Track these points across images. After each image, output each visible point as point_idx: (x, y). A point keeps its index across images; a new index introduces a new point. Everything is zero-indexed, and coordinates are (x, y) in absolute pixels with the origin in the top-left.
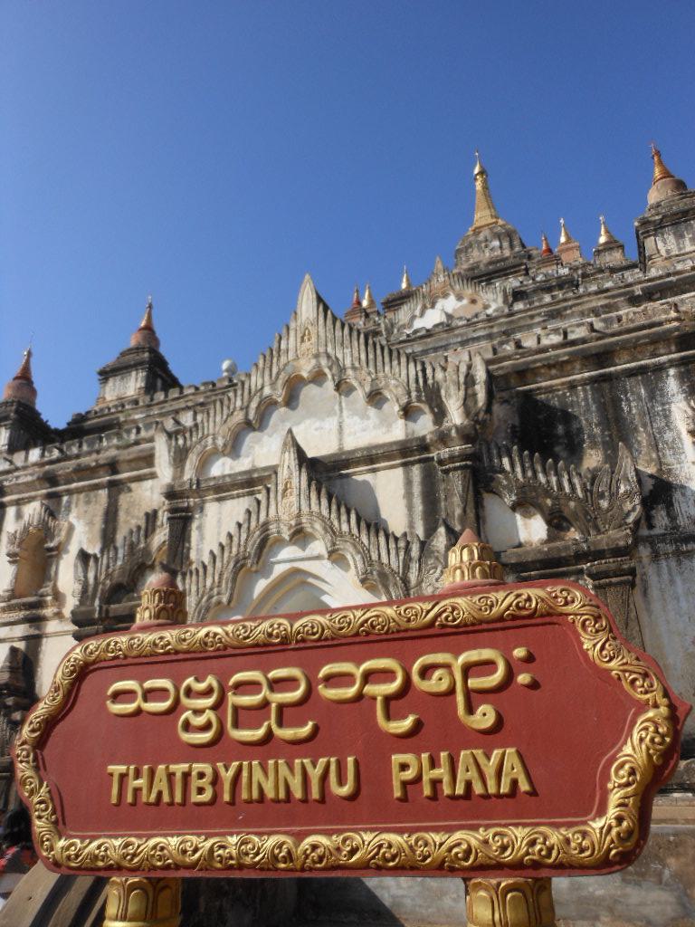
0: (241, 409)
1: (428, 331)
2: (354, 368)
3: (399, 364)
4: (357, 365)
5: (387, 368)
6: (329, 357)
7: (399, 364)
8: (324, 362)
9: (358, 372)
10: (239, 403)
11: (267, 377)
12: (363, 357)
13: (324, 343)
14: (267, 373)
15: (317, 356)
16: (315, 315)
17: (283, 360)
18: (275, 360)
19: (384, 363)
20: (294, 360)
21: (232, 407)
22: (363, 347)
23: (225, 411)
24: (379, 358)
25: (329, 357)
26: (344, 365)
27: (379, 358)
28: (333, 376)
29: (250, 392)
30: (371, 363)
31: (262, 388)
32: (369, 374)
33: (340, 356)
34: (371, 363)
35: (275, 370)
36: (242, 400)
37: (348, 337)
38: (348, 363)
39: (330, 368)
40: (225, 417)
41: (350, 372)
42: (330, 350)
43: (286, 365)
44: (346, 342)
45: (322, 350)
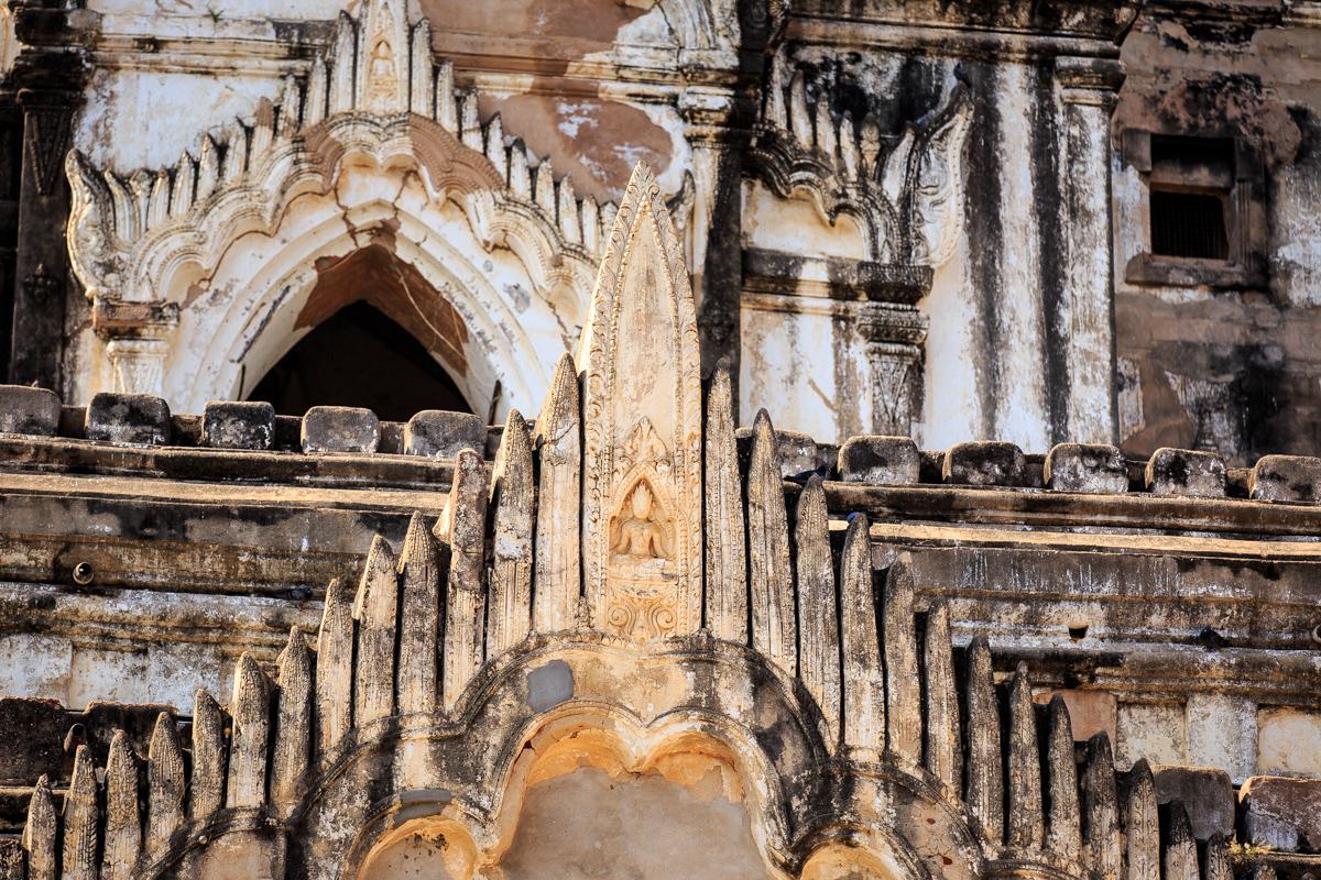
0: (263, 830)
1: (929, 470)
2: (903, 790)
3: (1122, 826)
4: (909, 766)
5: (1065, 832)
6: (761, 677)
7: (1122, 826)
8: (735, 697)
9: (919, 812)
10: (246, 792)
11: (415, 696)
12: (944, 732)
13: (735, 588)
14: (416, 662)
15: (700, 654)
16: (692, 424)
17: (511, 624)
18: (463, 605)
19: (1047, 803)
20: (570, 636)
21: (203, 807)
22: (943, 684)
23: (164, 825)
24: (1027, 772)
25: (761, 677)
26: (844, 749)
27: (1027, 772)
28: (786, 790)
29: (312, 750)
30: (985, 778)
31: (390, 742)
32: (972, 834)
33: (824, 694)
34: (985, 778)
35: (461, 668)
36: (269, 776)
37: (866, 603)
38: (864, 739)
39: (769, 742)
40: (159, 851)
41: (871, 797)
42: (772, 644)
43: (521, 652)
44: (858, 629)
45: (726, 626)
